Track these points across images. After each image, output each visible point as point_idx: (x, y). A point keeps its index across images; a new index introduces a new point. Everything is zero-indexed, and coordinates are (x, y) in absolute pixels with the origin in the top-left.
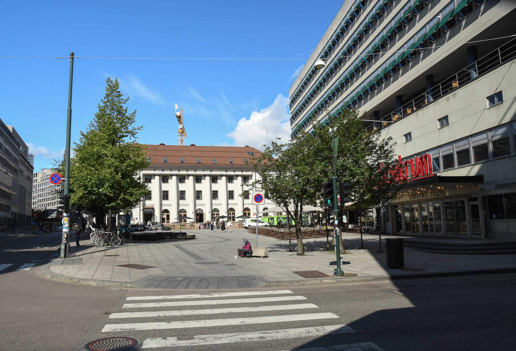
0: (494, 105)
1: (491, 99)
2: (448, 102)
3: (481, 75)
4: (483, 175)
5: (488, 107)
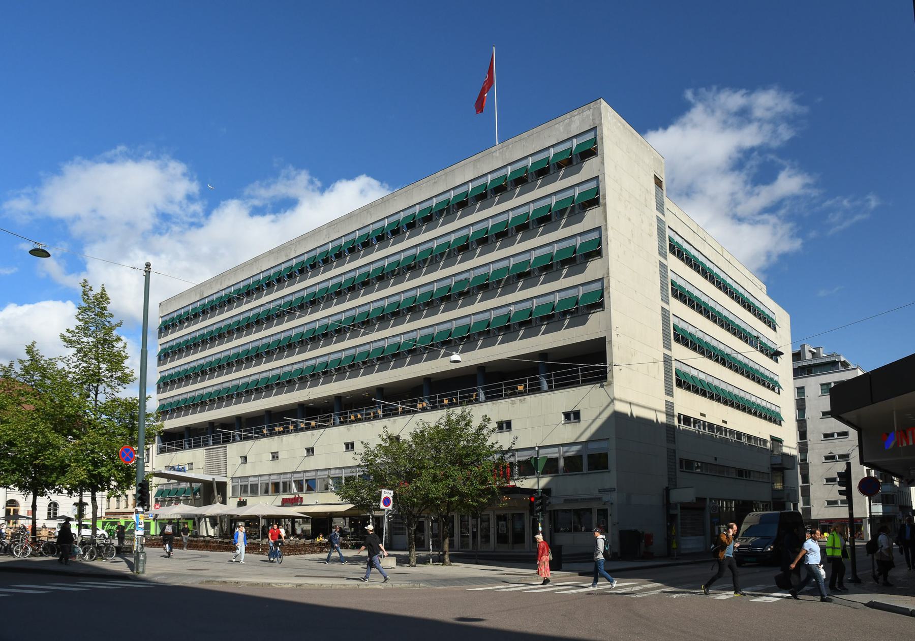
0: (569, 421)
1: (567, 415)
2: (513, 406)
3: (584, 384)
4: (550, 489)
5: (563, 423)
